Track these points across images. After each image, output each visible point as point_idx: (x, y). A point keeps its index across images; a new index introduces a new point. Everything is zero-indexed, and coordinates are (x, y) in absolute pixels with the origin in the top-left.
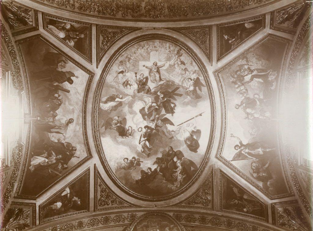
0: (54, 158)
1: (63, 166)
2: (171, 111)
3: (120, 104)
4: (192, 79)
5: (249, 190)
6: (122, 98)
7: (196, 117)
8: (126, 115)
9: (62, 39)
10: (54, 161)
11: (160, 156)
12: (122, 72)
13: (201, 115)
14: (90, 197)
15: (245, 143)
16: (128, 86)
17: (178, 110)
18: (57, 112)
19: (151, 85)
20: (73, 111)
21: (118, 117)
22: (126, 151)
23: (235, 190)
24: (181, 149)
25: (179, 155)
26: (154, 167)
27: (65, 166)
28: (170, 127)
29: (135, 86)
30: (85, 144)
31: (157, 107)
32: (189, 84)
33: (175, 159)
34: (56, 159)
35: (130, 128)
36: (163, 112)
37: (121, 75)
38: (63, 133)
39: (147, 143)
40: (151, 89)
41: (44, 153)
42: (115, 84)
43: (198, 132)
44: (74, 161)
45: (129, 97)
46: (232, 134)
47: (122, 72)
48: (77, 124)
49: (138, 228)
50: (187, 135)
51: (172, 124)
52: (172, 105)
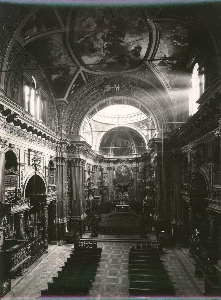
0: (61, 73)
1: (67, 77)
2: (123, 36)
3: (87, 38)
4: (137, 20)
5: (160, 81)
6: (87, 35)
7: (139, 40)
8: (93, 42)
9: (37, 31)
10: (62, 75)
11: (117, 56)
12: (84, 20)
13: (142, 39)
14: (84, 80)
15: (167, 56)
16: (91, 27)
17: (127, 36)
18: (51, 52)
19: (107, 22)
20: (60, 50)
21: (88, 44)
22: (97, 58)
23: (156, 78)
24: (129, 54)
25: (128, 57)
26: (113, 61)
27: (68, 76)
28: (122, 44)
29: (95, 25)
30: (73, 62)
31: (112, 34)
32: (135, 23)
33: (126, 58)
34: (62, 74)
35: (97, 48)
36: (117, 36)
37: (83, 22)
38: (59, 60)
39: (108, 52)
40: (107, 24)
41: (55, 73)
42: (81, 30)
43: (140, 48)
44: (71, 72)
45: (92, 32)
46: (160, 51)
47: (84, 20)
48: (65, 54)
49: (109, 83)
50: (133, 48)
51: (123, 42)
52: (123, 33)
